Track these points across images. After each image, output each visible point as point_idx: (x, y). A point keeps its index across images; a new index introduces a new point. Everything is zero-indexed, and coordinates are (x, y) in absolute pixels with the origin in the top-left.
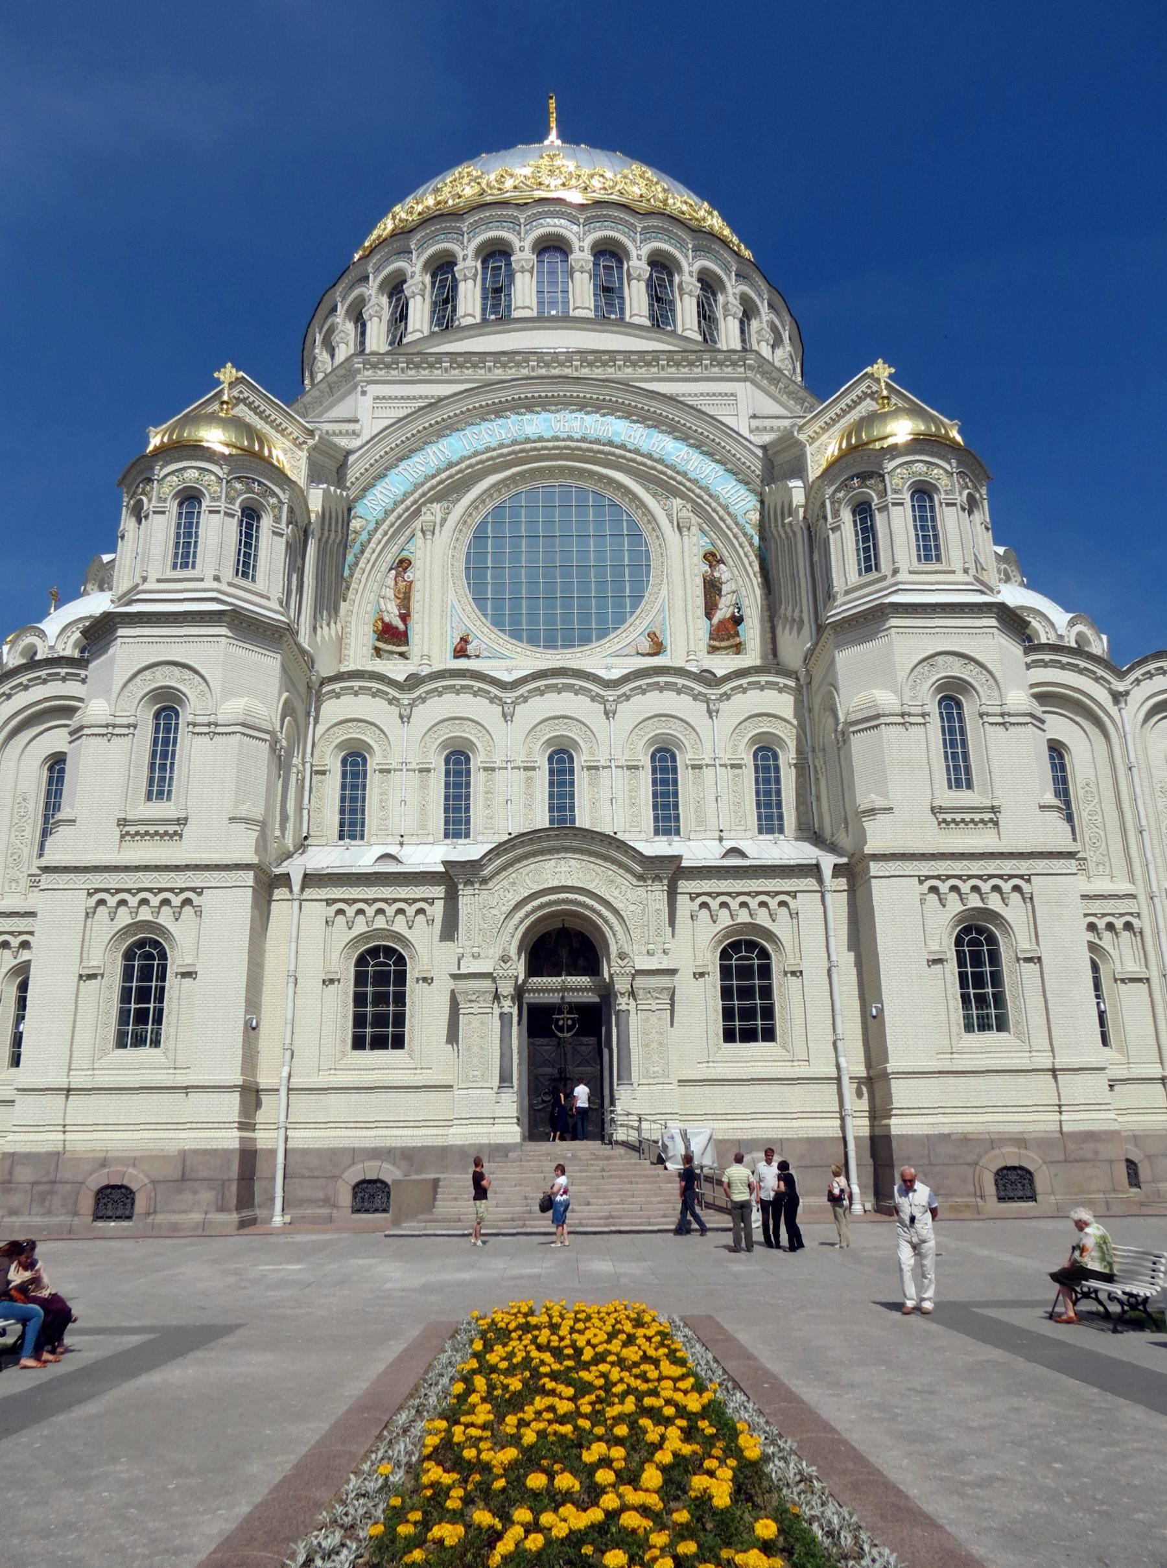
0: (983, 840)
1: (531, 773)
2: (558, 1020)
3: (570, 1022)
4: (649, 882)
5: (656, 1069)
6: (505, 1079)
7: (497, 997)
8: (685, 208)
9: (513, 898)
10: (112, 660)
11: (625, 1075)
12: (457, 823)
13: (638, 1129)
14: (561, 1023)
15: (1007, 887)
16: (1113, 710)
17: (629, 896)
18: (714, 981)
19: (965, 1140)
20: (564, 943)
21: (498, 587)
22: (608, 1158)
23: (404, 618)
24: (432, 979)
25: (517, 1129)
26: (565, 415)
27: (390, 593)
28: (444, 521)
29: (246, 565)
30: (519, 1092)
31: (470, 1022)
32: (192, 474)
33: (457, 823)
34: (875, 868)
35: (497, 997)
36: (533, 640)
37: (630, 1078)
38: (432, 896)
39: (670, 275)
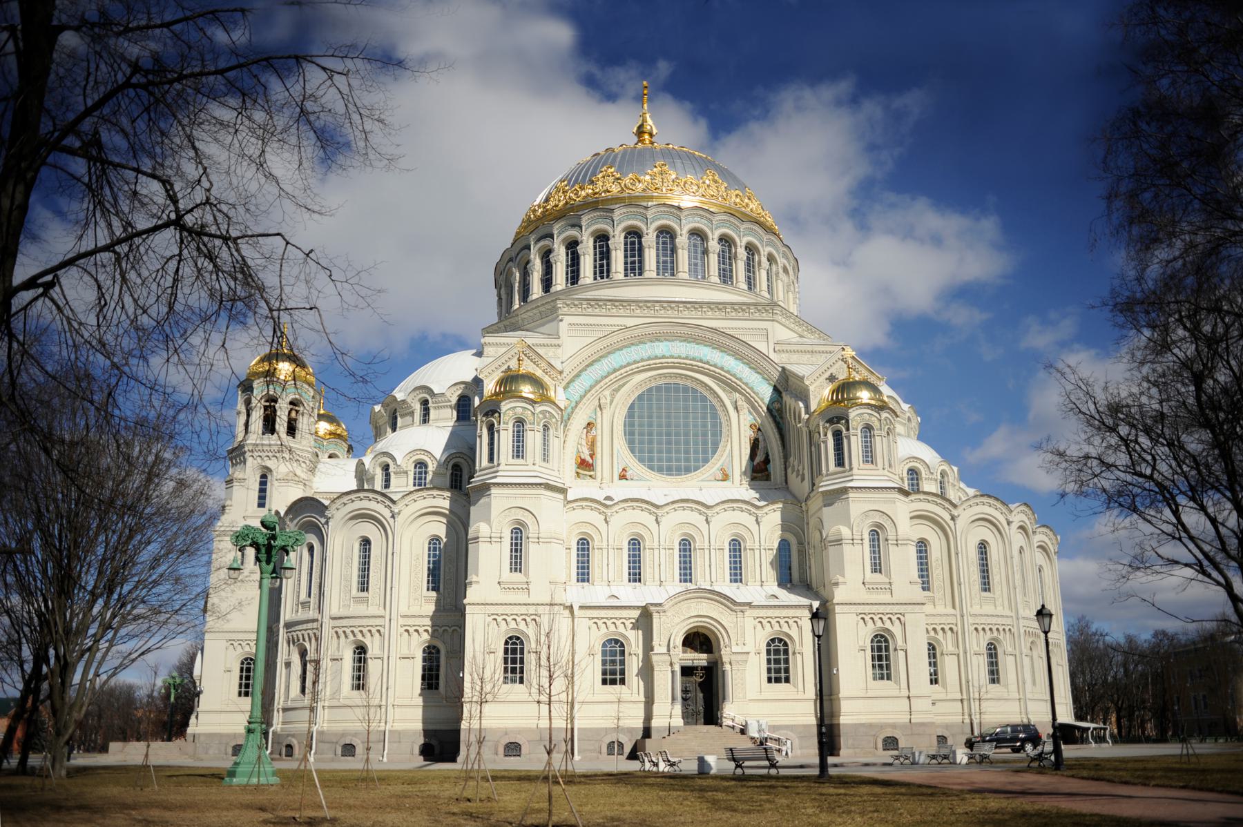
0: (886, 597)
8: (738, 200)
10: (489, 505)
12: (635, 576)
15: (894, 618)
16: (951, 523)
18: (764, 656)
19: (871, 725)
21: (641, 442)
23: (592, 456)
26: (678, 343)
27: (584, 442)
28: (612, 402)
29: (545, 458)
32: (519, 410)
33: (635, 576)
34: (838, 609)
36: (660, 470)
39: (730, 246)
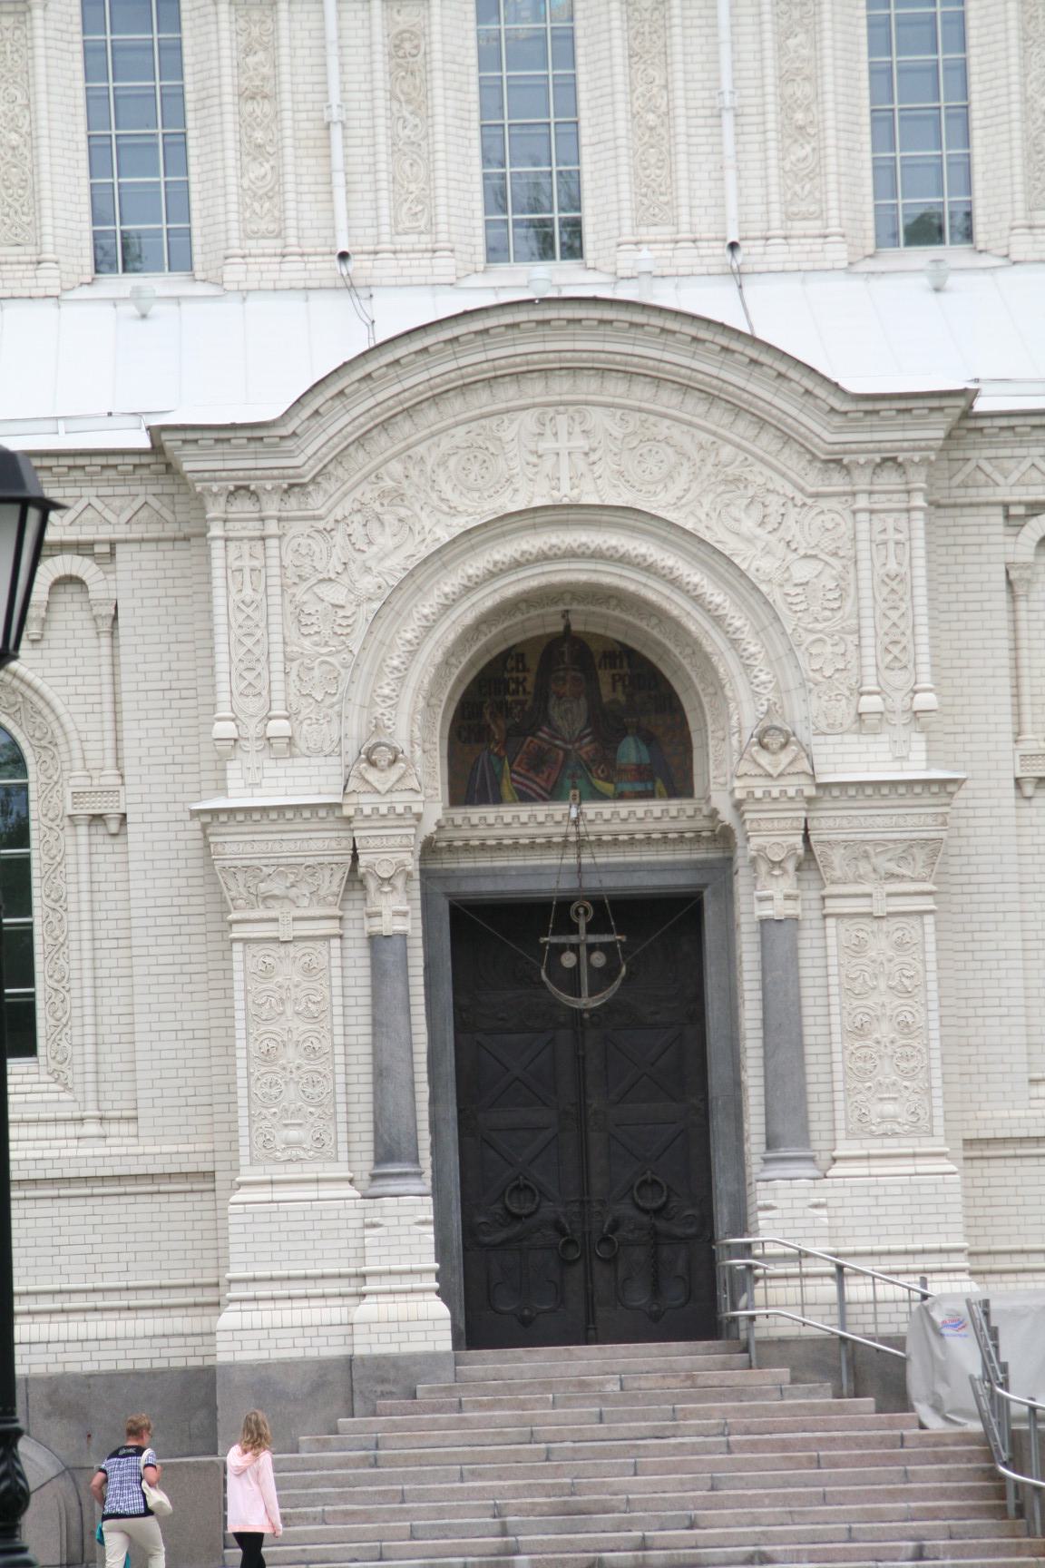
2: (559, 950)
3: (599, 959)
5: (889, 1108)
6: (389, 1151)
7: (355, 879)
9: (392, 553)
11: (791, 1134)
14: (568, 960)
17: (792, 529)
20: (568, 691)
22: (738, 1393)
25: (440, 1310)
30: (437, 1192)
31: (268, 972)
35: (355, 879)
37: (804, 1137)
38: (105, 533)
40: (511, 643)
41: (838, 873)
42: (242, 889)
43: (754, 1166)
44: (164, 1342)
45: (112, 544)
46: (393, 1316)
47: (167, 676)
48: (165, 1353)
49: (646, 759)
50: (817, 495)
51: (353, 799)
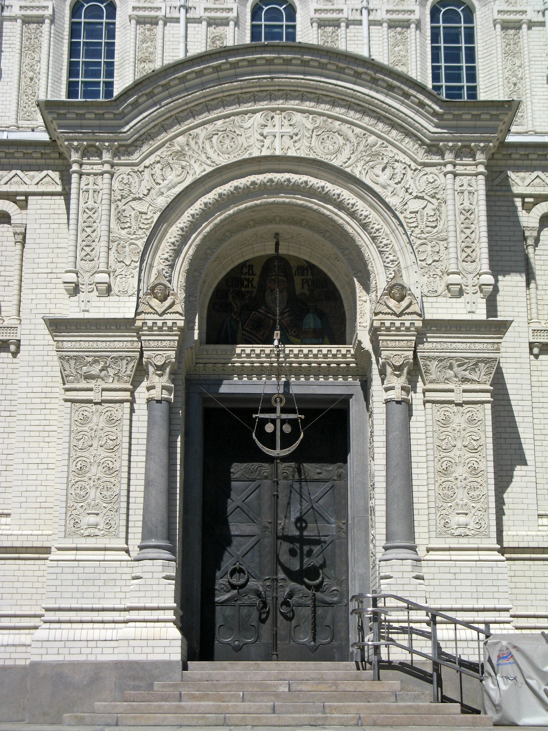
1: (221, 30)
2: (264, 422)
3: (287, 428)
4: (449, 157)
9: (175, 181)
11: (402, 532)
13: (431, 636)
14: (269, 428)
17: (409, 181)
22: (367, 696)
24: (18, 343)
25: (176, 633)
31: (85, 420)
38: (23, 188)
40: (246, 258)
41: (433, 377)
42: (73, 370)
43: (380, 553)
44: (12, 649)
45: (27, 195)
46: (144, 636)
47: (50, 265)
48: (13, 656)
49: (319, 325)
50: (425, 165)
51: (142, 316)
